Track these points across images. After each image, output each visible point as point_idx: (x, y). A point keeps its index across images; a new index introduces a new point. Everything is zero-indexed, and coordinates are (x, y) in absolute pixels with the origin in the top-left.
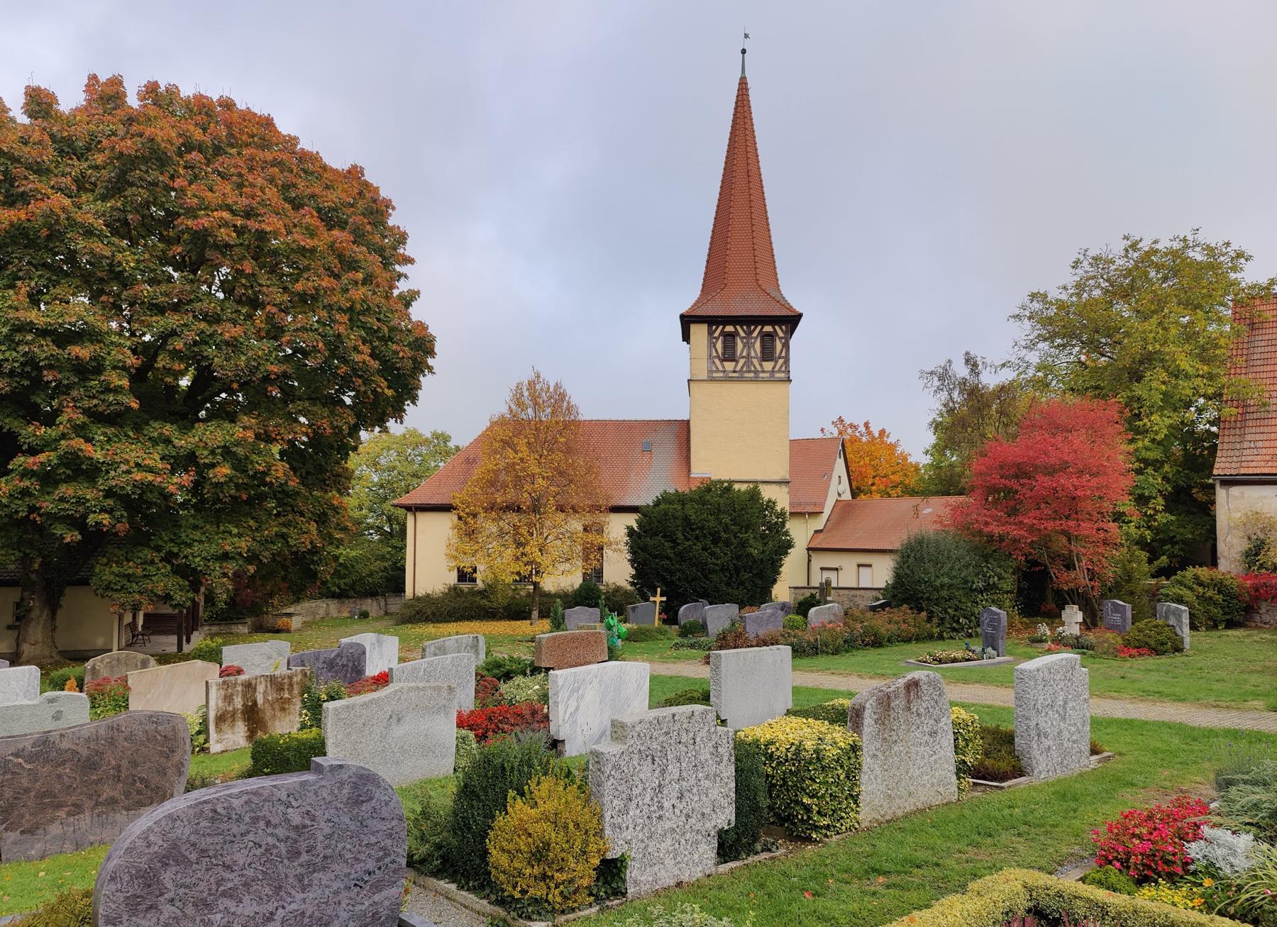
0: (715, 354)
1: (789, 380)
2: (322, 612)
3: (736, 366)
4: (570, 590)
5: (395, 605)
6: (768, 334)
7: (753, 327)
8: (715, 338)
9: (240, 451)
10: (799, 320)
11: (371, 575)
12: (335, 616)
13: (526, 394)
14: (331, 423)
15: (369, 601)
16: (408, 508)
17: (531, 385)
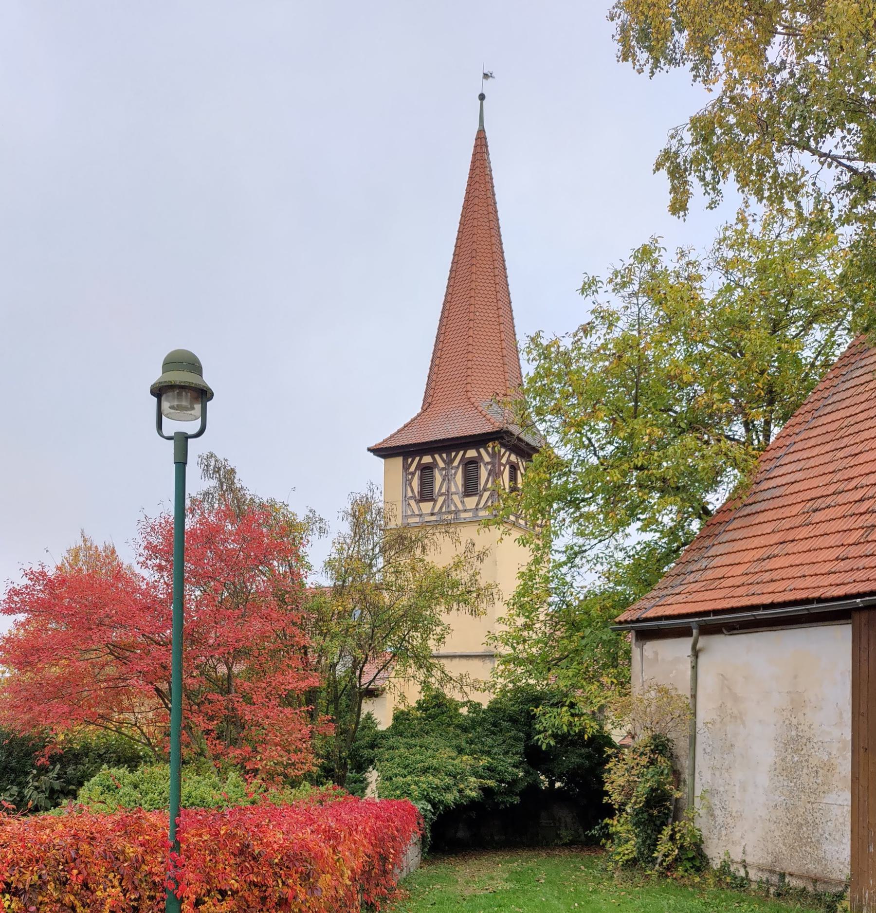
0: (410, 494)
8: (410, 473)
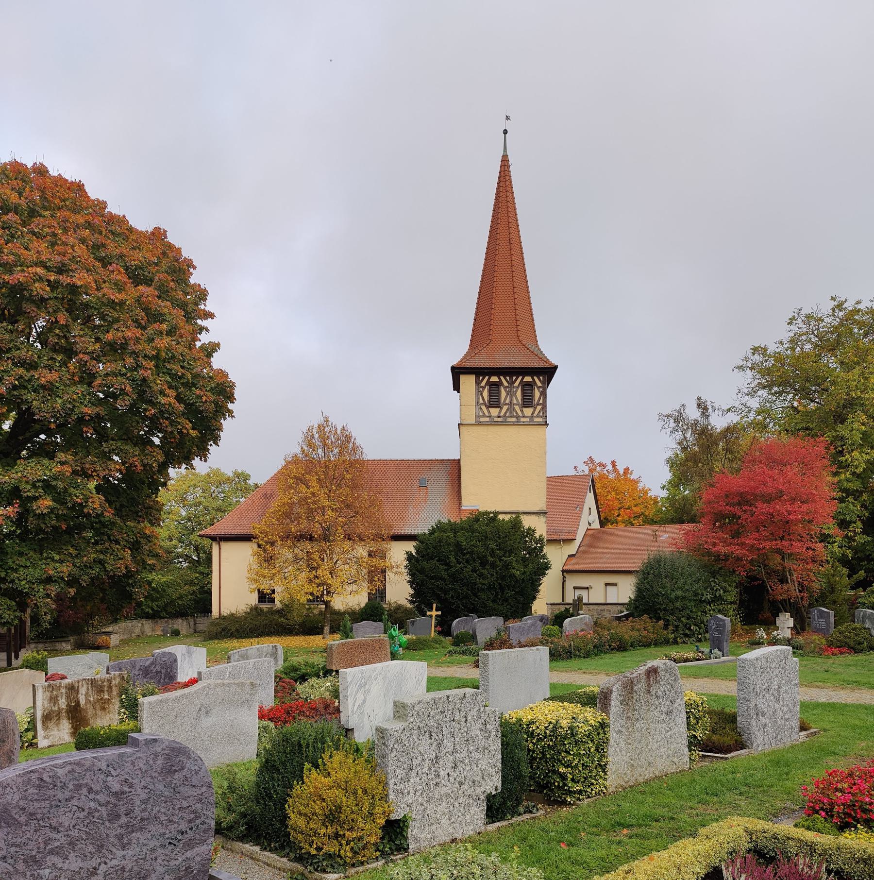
0: (481, 401)
1: (546, 424)
2: (137, 631)
3: (500, 412)
4: (357, 608)
5: (203, 624)
6: (528, 384)
7: (514, 378)
9: (60, 485)
10: (555, 372)
11: (181, 598)
12: (150, 634)
13: (316, 436)
14: (142, 461)
15: (180, 621)
16: (213, 538)
17: (321, 428)
